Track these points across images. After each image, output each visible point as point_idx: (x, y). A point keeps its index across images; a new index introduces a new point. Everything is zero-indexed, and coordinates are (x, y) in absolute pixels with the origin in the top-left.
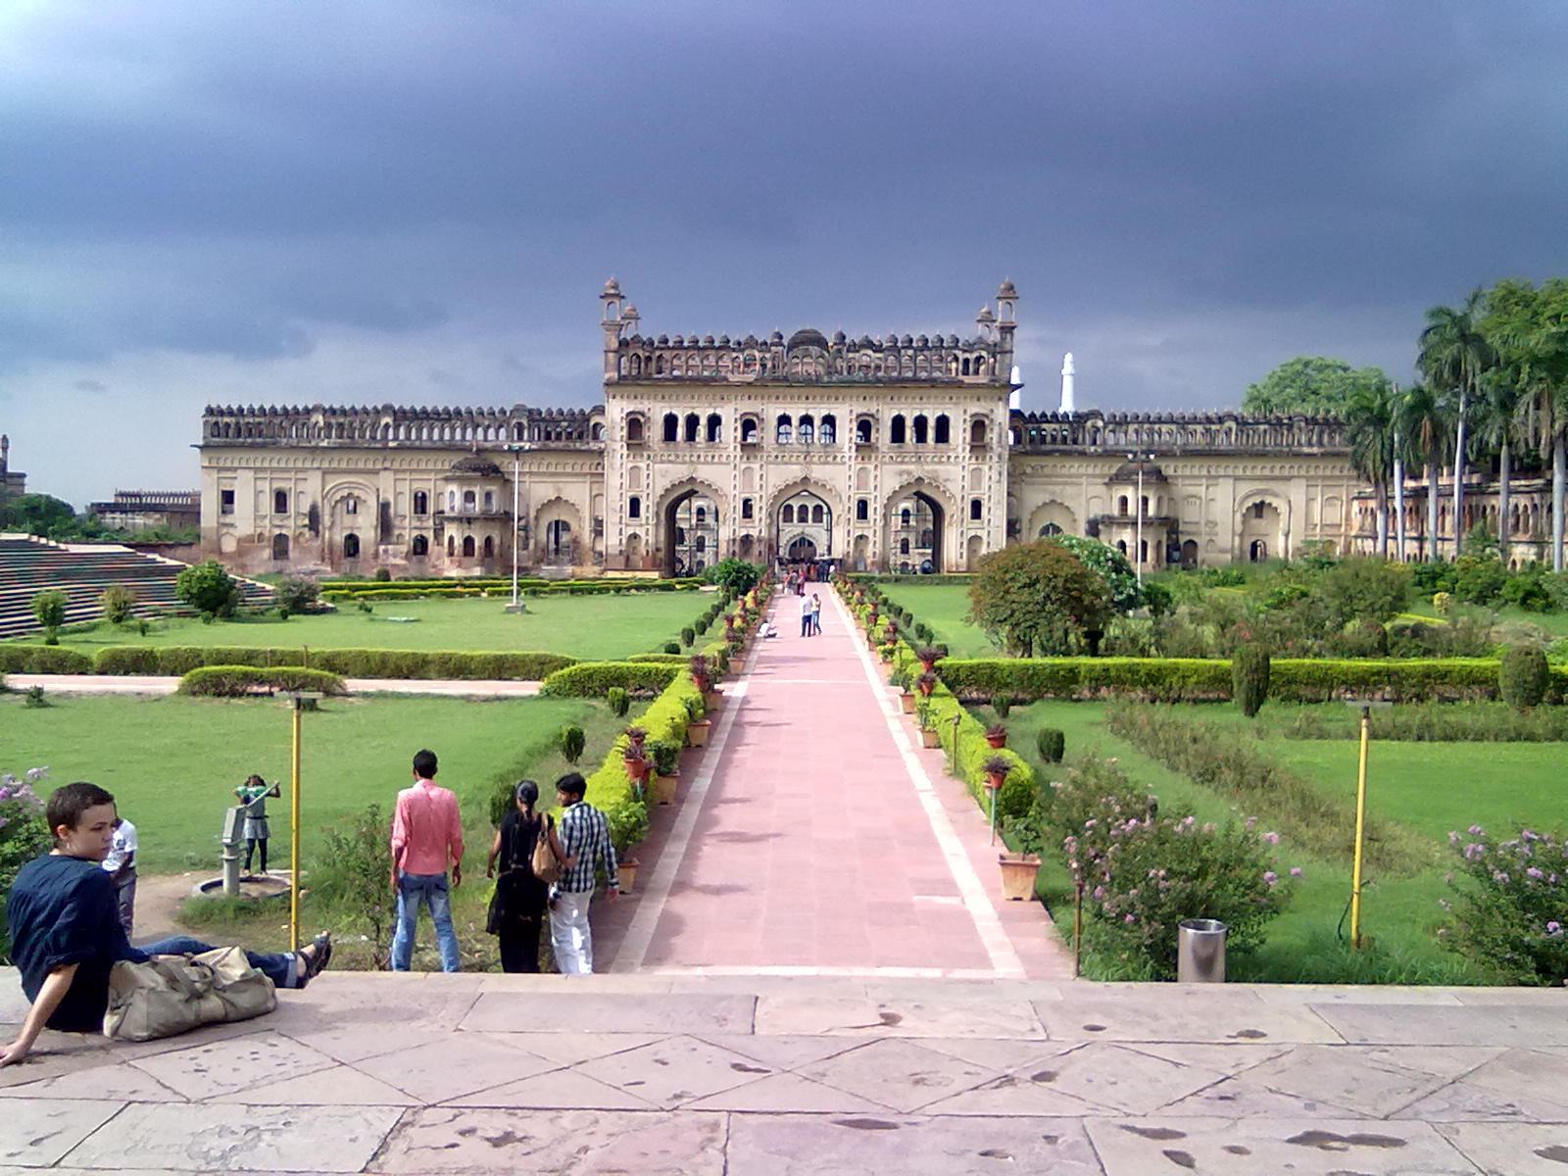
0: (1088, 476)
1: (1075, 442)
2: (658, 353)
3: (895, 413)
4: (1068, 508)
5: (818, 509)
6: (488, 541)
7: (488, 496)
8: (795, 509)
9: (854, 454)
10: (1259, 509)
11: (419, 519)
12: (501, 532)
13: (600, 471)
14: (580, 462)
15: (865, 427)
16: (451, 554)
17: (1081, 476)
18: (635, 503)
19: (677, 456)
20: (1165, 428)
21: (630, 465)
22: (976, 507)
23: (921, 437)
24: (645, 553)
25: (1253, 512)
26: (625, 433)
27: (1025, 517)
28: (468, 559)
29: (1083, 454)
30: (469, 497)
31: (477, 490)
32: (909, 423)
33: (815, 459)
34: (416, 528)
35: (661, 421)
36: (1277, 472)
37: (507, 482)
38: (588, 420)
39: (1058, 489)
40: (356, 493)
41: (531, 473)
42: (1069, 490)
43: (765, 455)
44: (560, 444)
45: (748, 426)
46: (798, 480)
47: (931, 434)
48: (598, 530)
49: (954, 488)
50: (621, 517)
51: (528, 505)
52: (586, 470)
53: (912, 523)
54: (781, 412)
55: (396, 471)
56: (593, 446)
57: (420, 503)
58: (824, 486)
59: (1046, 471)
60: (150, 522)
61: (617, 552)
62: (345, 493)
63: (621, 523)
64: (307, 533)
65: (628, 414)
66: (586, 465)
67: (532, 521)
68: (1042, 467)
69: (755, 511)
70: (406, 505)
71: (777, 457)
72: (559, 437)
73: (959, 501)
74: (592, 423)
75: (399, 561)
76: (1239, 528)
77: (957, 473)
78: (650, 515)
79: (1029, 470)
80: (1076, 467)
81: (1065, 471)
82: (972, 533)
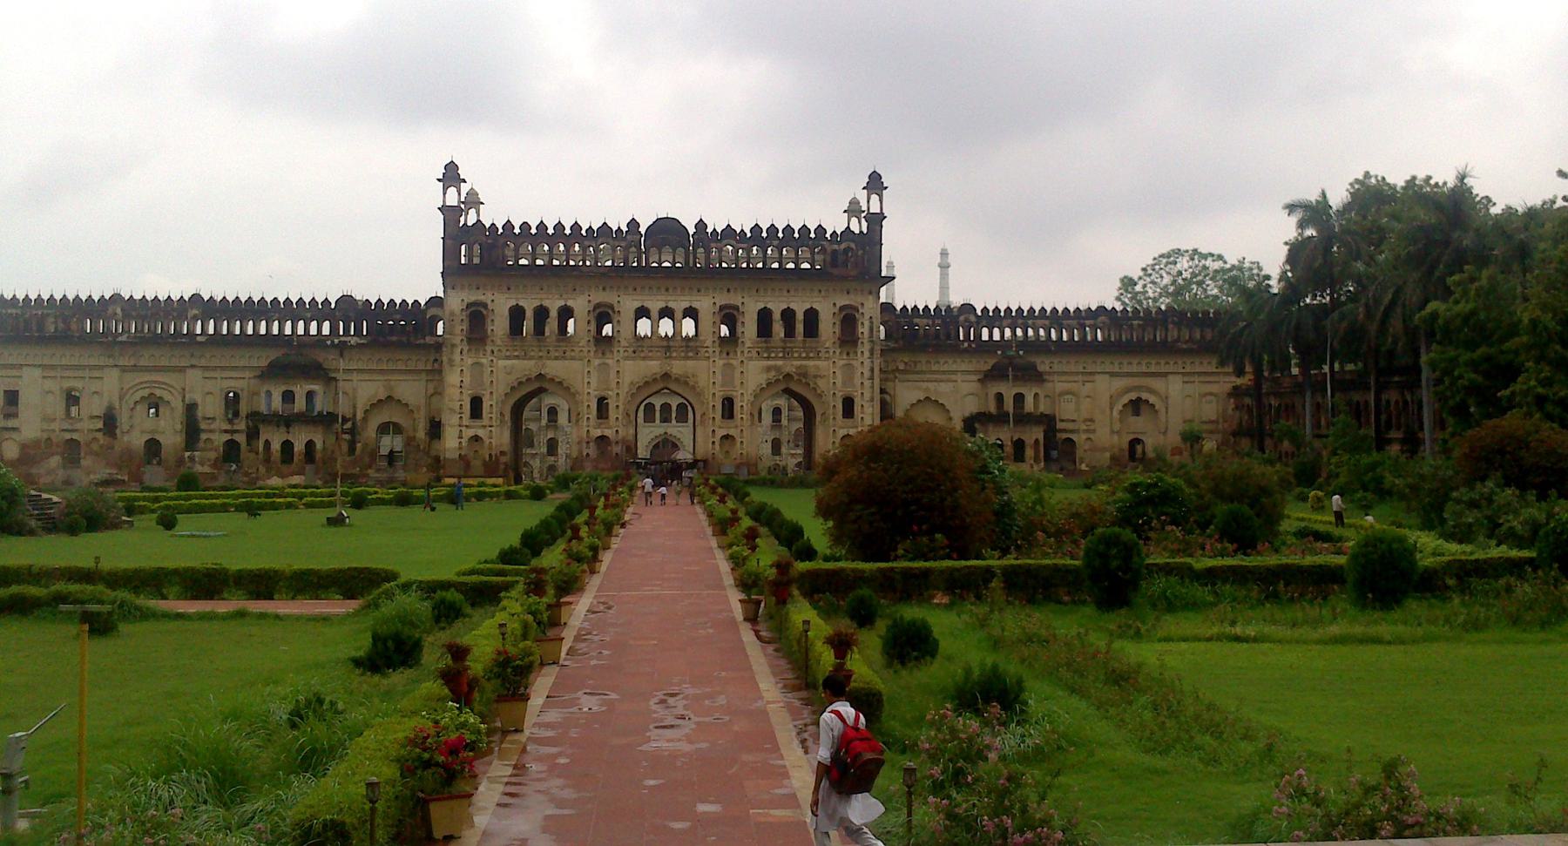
2: (502, 241)
5: (682, 409)
6: (310, 445)
7: (310, 395)
8: (658, 408)
9: (718, 350)
10: (1136, 406)
11: (230, 421)
14: (414, 358)
15: (729, 316)
16: (267, 460)
20: (1039, 322)
21: (470, 361)
22: (848, 406)
23: (790, 332)
25: (1130, 410)
28: (285, 468)
30: (288, 397)
32: (777, 316)
34: (226, 431)
35: (507, 313)
36: (1153, 369)
39: (931, 386)
40: (158, 393)
42: (944, 387)
44: (394, 338)
45: (603, 315)
47: (800, 328)
48: (435, 429)
51: (355, 407)
53: (784, 422)
54: (637, 304)
55: (206, 368)
56: (429, 340)
57: (232, 403)
58: (686, 383)
59: (919, 368)
62: (146, 393)
64: (99, 435)
65: (469, 305)
66: (420, 362)
69: (612, 414)
70: (211, 407)
75: (207, 469)
76: (1117, 427)
79: (901, 367)
81: (934, 368)
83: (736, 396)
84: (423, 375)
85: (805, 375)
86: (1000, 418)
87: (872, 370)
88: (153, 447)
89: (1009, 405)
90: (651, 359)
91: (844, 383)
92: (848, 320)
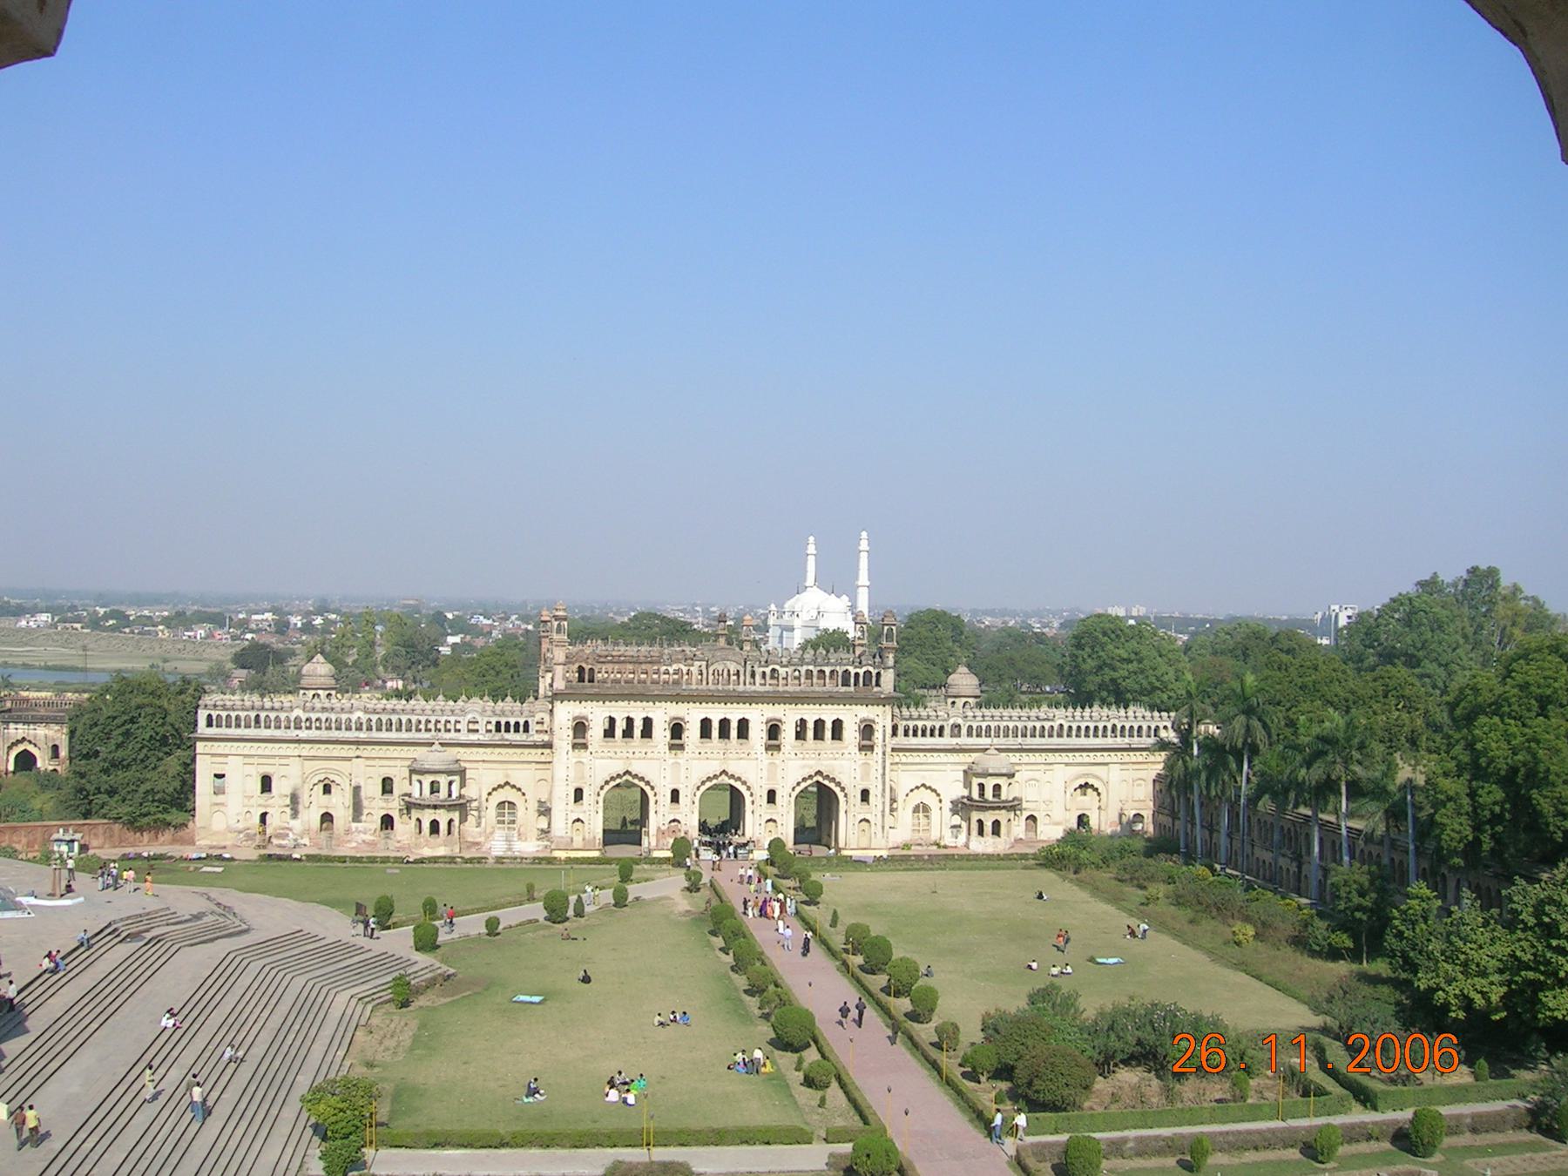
6: (451, 821)
22: (865, 795)
23: (819, 735)
26: (571, 733)
27: (900, 798)
30: (434, 788)
31: (443, 780)
37: (462, 773)
40: (332, 777)
48: (545, 810)
56: (538, 738)
60: (50, 733)
66: (535, 754)
67: (484, 804)
70: (372, 789)
72: (507, 730)
88: (327, 818)
89: (989, 794)
92: (867, 730)
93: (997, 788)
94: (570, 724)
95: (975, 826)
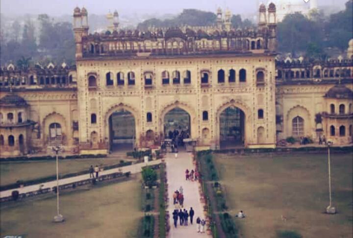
0: (315, 93)
1: (308, 76)
3: (219, 69)
4: (306, 109)
6: (21, 137)
7: (20, 114)
9: (200, 89)
12: (27, 131)
13: (74, 98)
17: (311, 93)
18: (94, 118)
19: (114, 93)
21: (90, 98)
22: (261, 113)
23: (232, 78)
24: (99, 141)
26: (87, 82)
27: (285, 114)
29: (312, 83)
30: (10, 116)
31: (15, 113)
33: (181, 92)
38: (67, 74)
39: (300, 100)
41: (40, 101)
42: (305, 100)
43: (157, 91)
44: (54, 86)
46: (174, 103)
47: (237, 78)
48: (76, 126)
49: (249, 104)
50: (87, 124)
51: (39, 117)
52: (67, 98)
56: (71, 86)
59: (294, 91)
61: (86, 141)
63: (87, 127)
65: (89, 74)
66: (67, 96)
68: (292, 90)
71: (162, 92)
72: (53, 83)
73: (252, 110)
74: (69, 75)
77: (251, 97)
78: (101, 122)
79: (286, 91)
80: (308, 89)
81: (303, 91)
82: (258, 126)
83: (209, 110)
84: (69, 102)
85: (240, 100)
86: (332, 116)
87: (272, 97)
90: (170, 95)
91: (259, 104)
92: (260, 74)
93: (342, 107)
94: (87, 78)
95: (329, 129)
